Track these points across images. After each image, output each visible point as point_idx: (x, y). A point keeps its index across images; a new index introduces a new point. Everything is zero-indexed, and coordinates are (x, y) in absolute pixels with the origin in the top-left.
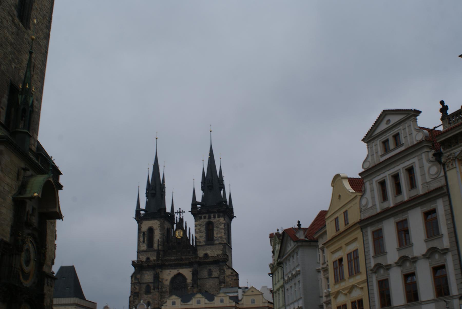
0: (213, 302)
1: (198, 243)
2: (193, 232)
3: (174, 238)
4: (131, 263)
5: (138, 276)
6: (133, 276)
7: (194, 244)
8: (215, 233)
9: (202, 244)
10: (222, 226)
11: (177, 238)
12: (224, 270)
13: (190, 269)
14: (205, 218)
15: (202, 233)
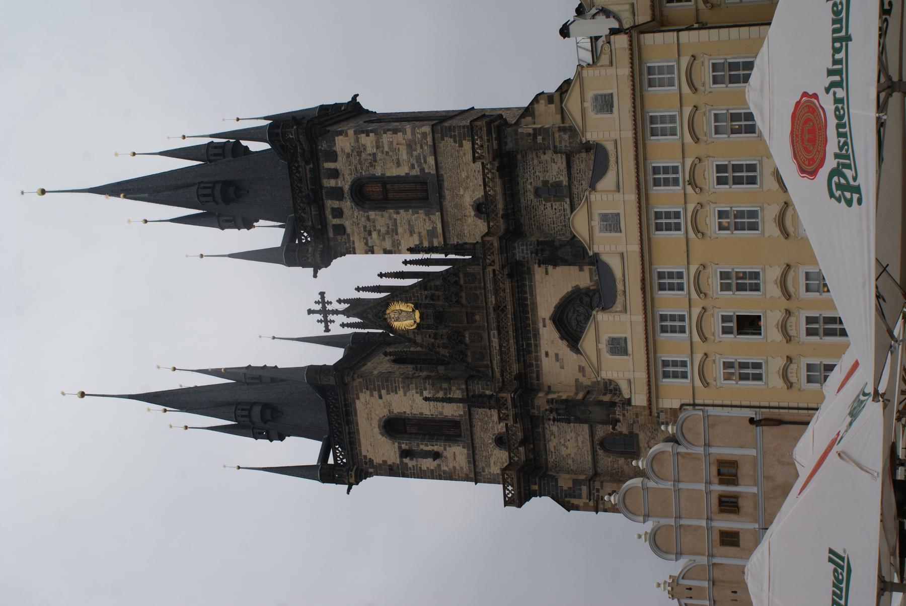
0: (610, 147)
1: (436, 244)
2: (395, 262)
3: (419, 339)
4: (512, 509)
5: (565, 482)
6: (567, 502)
7: (442, 256)
8: (393, 171)
9: (439, 226)
10: (368, 141)
11: (419, 326)
12: (536, 132)
13: (538, 272)
14: (338, 213)
15: (396, 225)
